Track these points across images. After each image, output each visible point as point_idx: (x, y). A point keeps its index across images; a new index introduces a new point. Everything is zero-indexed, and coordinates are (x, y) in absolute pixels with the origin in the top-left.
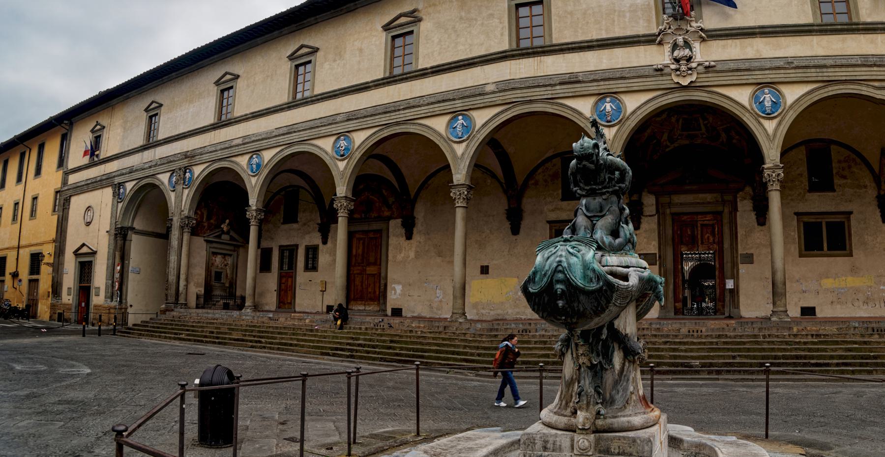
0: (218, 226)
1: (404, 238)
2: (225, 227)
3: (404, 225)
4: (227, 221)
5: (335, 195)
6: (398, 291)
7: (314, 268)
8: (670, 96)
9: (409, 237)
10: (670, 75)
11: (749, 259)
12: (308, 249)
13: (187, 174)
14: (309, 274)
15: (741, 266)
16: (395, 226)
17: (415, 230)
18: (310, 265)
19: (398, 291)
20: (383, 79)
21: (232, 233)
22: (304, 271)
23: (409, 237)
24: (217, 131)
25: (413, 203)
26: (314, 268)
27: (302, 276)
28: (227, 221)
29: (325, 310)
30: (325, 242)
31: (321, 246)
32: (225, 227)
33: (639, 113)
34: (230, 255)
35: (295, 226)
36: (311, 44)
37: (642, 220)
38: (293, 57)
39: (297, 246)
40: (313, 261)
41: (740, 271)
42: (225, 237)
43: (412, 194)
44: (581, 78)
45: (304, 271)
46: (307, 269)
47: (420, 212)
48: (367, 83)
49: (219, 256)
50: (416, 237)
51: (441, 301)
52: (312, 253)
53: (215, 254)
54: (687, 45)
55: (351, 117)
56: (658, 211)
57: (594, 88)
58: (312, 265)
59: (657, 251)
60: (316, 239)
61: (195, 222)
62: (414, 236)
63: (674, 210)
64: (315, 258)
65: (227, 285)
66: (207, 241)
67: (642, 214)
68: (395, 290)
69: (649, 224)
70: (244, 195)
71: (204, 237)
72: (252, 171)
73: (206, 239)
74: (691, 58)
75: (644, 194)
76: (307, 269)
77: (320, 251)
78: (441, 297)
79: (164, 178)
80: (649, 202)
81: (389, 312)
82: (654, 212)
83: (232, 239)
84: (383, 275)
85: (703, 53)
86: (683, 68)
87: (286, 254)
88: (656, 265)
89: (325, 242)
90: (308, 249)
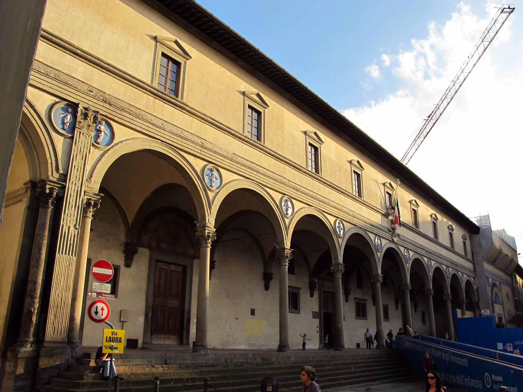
22: (356, 319)
30: (128, 265)
45: (356, 319)
51: (228, 335)
63: (325, 289)
69: (316, 295)
77: (121, 274)
78: (228, 332)
84: (186, 309)
88: (318, 318)
89: (128, 265)
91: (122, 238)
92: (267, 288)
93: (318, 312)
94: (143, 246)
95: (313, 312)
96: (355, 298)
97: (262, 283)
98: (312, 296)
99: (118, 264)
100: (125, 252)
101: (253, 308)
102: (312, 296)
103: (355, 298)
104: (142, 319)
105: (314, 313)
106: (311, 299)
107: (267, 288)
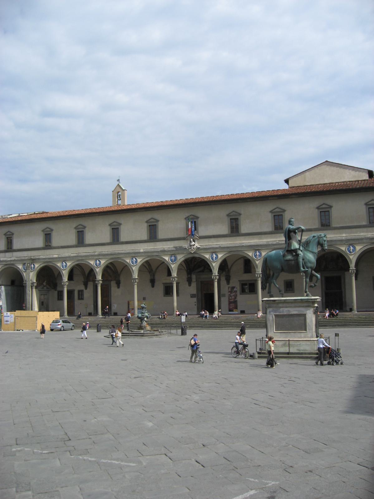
0: (42, 284)
1: (117, 288)
2: (45, 284)
3: (116, 283)
4: (45, 281)
6: (115, 307)
7: (82, 299)
8: (189, 255)
9: (118, 287)
10: (189, 249)
12: (79, 291)
14: (80, 301)
15: (221, 298)
17: (121, 285)
18: (80, 298)
19: (115, 307)
20: (110, 243)
21: (48, 286)
23: (118, 287)
24: (45, 250)
25: (119, 275)
26: (82, 299)
27: (77, 302)
28: (45, 281)
29: (88, 314)
31: (85, 291)
32: (45, 284)
33: (181, 260)
34: (46, 294)
37: (192, 283)
38: (77, 228)
39: (74, 290)
41: (222, 299)
42: (45, 288)
43: (119, 273)
44: (166, 250)
46: (79, 299)
47: (122, 279)
49: (43, 295)
50: (121, 287)
52: (81, 293)
53: (41, 295)
54: (194, 241)
56: (196, 281)
57: (169, 253)
58: (81, 297)
60: (82, 287)
61: (36, 284)
64: (82, 295)
65: (46, 307)
66: (39, 290)
67: (191, 280)
68: (114, 306)
69: (194, 285)
70: (60, 275)
71: (38, 289)
72: (63, 267)
73: (39, 289)
74: (194, 245)
75: (192, 275)
76: (79, 299)
79: (20, 267)
80: (194, 277)
81: (113, 314)
82: (195, 280)
83: (47, 288)
85: (197, 245)
86: (192, 248)
88: (196, 297)
89: (86, 289)
90: (79, 291)
91: (83, 280)
92: (153, 286)
93: (195, 294)
94: (90, 281)
95: (191, 294)
96: (239, 281)
97: (150, 284)
98: (190, 285)
99: (83, 289)
100: (84, 284)
101: (144, 297)
102: (190, 285)
103: (239, 281)
104: (92, 306)
106: (189, 287)
107: (153, 286)
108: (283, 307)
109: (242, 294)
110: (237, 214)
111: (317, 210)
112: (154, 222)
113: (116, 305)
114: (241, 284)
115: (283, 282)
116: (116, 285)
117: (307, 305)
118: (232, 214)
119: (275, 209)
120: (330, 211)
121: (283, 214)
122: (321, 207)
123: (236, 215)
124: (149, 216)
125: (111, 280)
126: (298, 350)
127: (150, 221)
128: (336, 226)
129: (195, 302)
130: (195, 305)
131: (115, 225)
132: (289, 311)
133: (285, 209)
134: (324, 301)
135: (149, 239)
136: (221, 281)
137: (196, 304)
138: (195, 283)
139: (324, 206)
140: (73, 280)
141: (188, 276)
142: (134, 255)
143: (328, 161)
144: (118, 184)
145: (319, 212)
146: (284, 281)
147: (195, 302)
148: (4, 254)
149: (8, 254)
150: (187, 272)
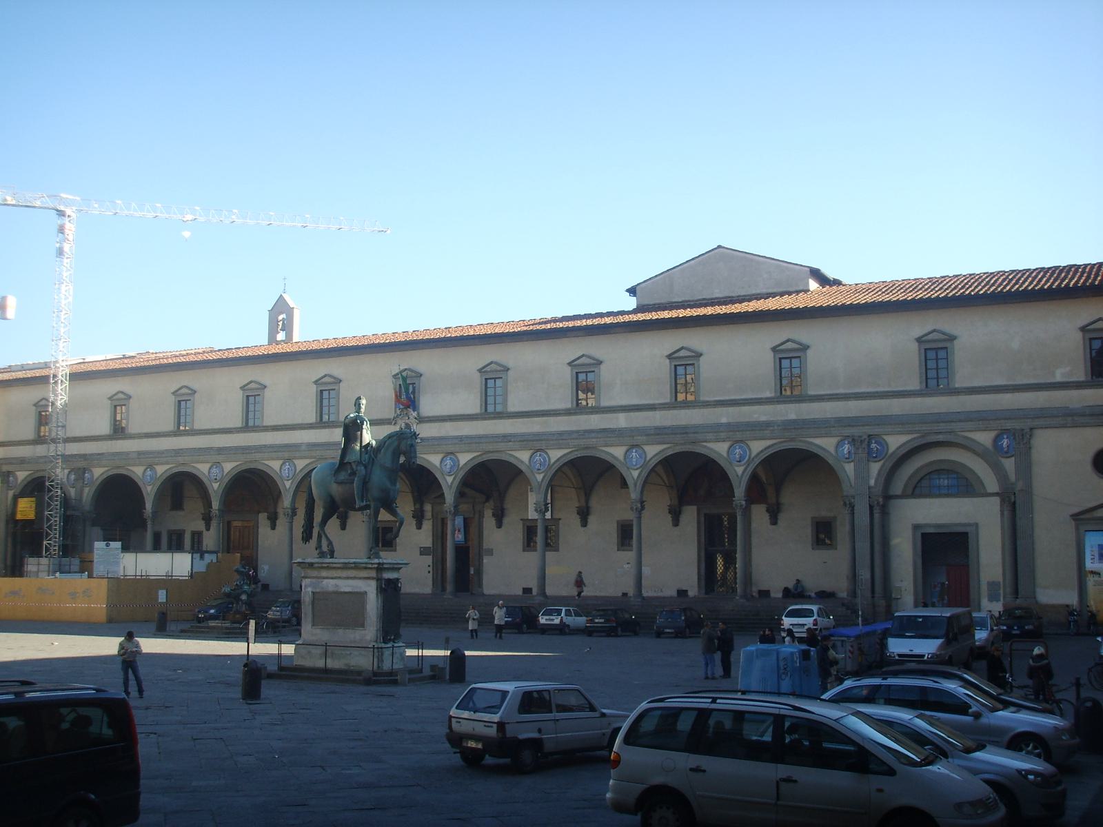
1: (270, 528)
3: (268, 518)
5: (212, 508)
11: (490, 552)
13: (86, 475)
16: (263, 517)
20: (241, 428)
31: (205, 533)
35: (181, 513)
36: (190, 385)
39: (184, 531)
40: (198, 544)
41: (485, 561)
48: (231, 429)
55: (220, 450)
56: (432, 515)
59: (431, 546)
60: (200, 525)
62: (277, 527)
64: (200, 542)
68: (264, 569)
69: (427, 525)
80: (428, 508)
87: (174, 537)
89: (208, 529)
95: (421, 548)
98: (419, 527)
100: (203, 519)
102: (419, 527)
103: (521, 520)
105: (422, 549)
106: (417, 531)
108: (327, 578)
109: (528, 551)
110: (499, 368)
111: (668, 361)
112: (330, 383)
113: (266, 567)
114: (526, 527)
115: (616, 525)
116: (268, 523)
117: (366, 575)
118: (488, 369)
119: (578, 358)
120: (696, 365)
121: (596, 370)
122: (676, 355)
123: (497, 371)
124: (321, 368)
125: (259, 512)
126: (346, 665)
127: (323, 380)
128: (707, 399)
129: (429, 566)
130: (429, 572)
131: (251, 389)
132: (337, 586)
133: (601, 359)
134: (703, 571)
135: (112, 431)
136: (484, 519)
137: (431, 569)
138: (431, 520)
139: (682, 353)
140: (183, 510)
141: (415, 504)
142: (286, 455)
143: (723, 245)
144: (281, 295)
145: (673, 367)
146: (618, 522)
147: (429, 566)
148: (31, 447)
149: (40, 450)
150: (413, 497)
